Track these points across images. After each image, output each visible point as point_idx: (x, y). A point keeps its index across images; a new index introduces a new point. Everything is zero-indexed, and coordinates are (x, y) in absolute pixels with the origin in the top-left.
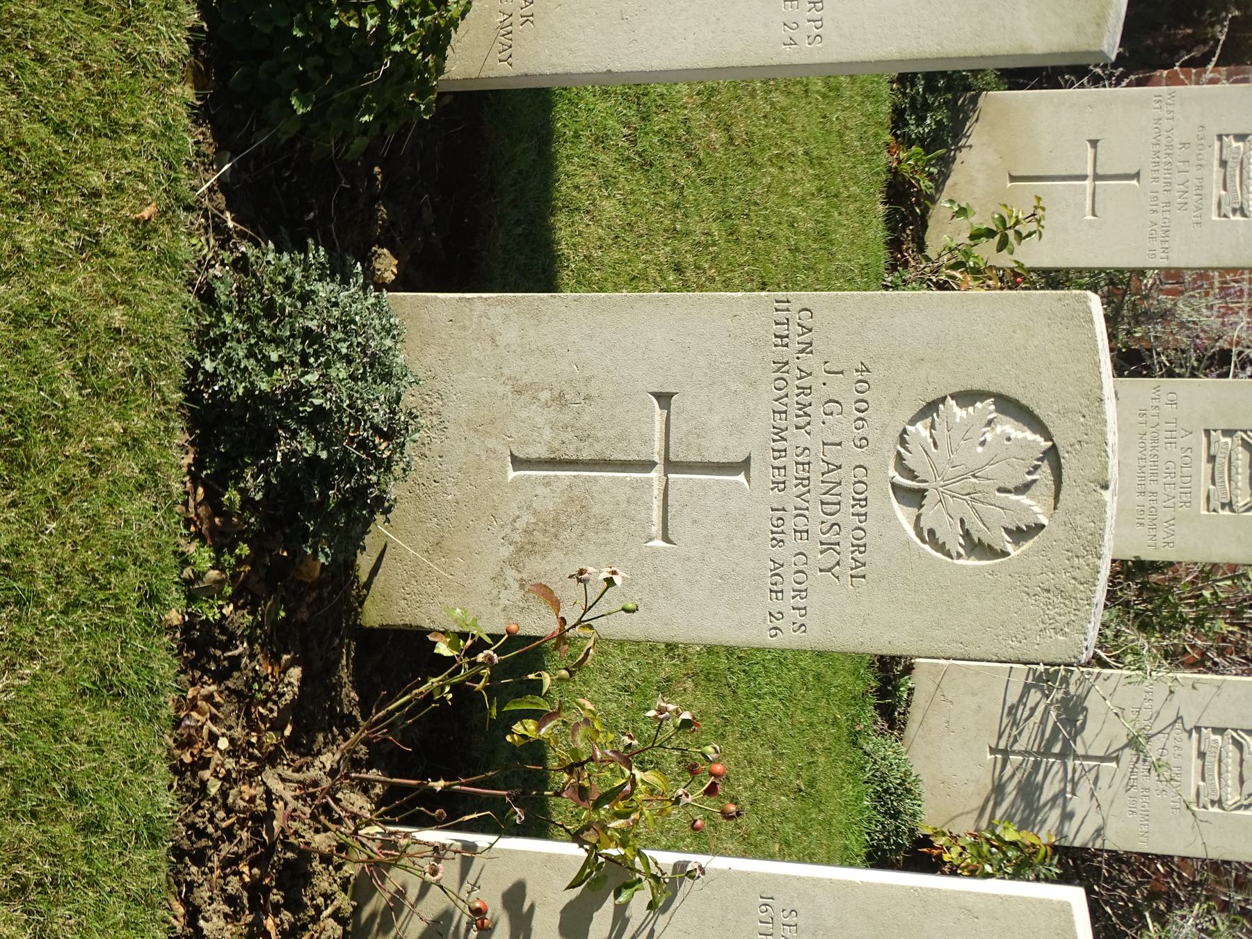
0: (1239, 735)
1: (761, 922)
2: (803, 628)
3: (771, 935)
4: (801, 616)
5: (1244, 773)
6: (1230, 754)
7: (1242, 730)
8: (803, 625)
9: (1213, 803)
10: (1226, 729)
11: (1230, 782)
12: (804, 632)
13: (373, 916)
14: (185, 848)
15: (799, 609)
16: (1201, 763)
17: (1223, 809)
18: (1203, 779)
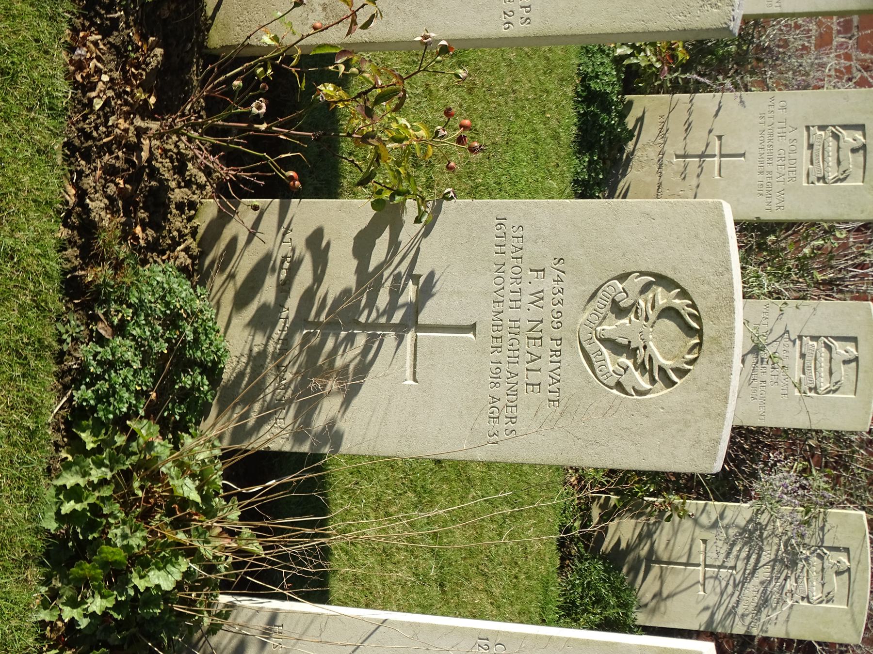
0: (837, 130)
1: (497, 237)
2: (528, 21)
3: (504, 245)
4: (527, 12)
5: (832, 367)
6: (823, 354)
7: (831, 337)
8: (528, 18)
9: (819, 179)
10: (827, 126)
11: (822, 374)
12: (529, 23)
13: (213, 262)
14: (77, 144)
15: (525, 7)
16: (802, 361)
17: (826, 183)
18: (804, 373)
